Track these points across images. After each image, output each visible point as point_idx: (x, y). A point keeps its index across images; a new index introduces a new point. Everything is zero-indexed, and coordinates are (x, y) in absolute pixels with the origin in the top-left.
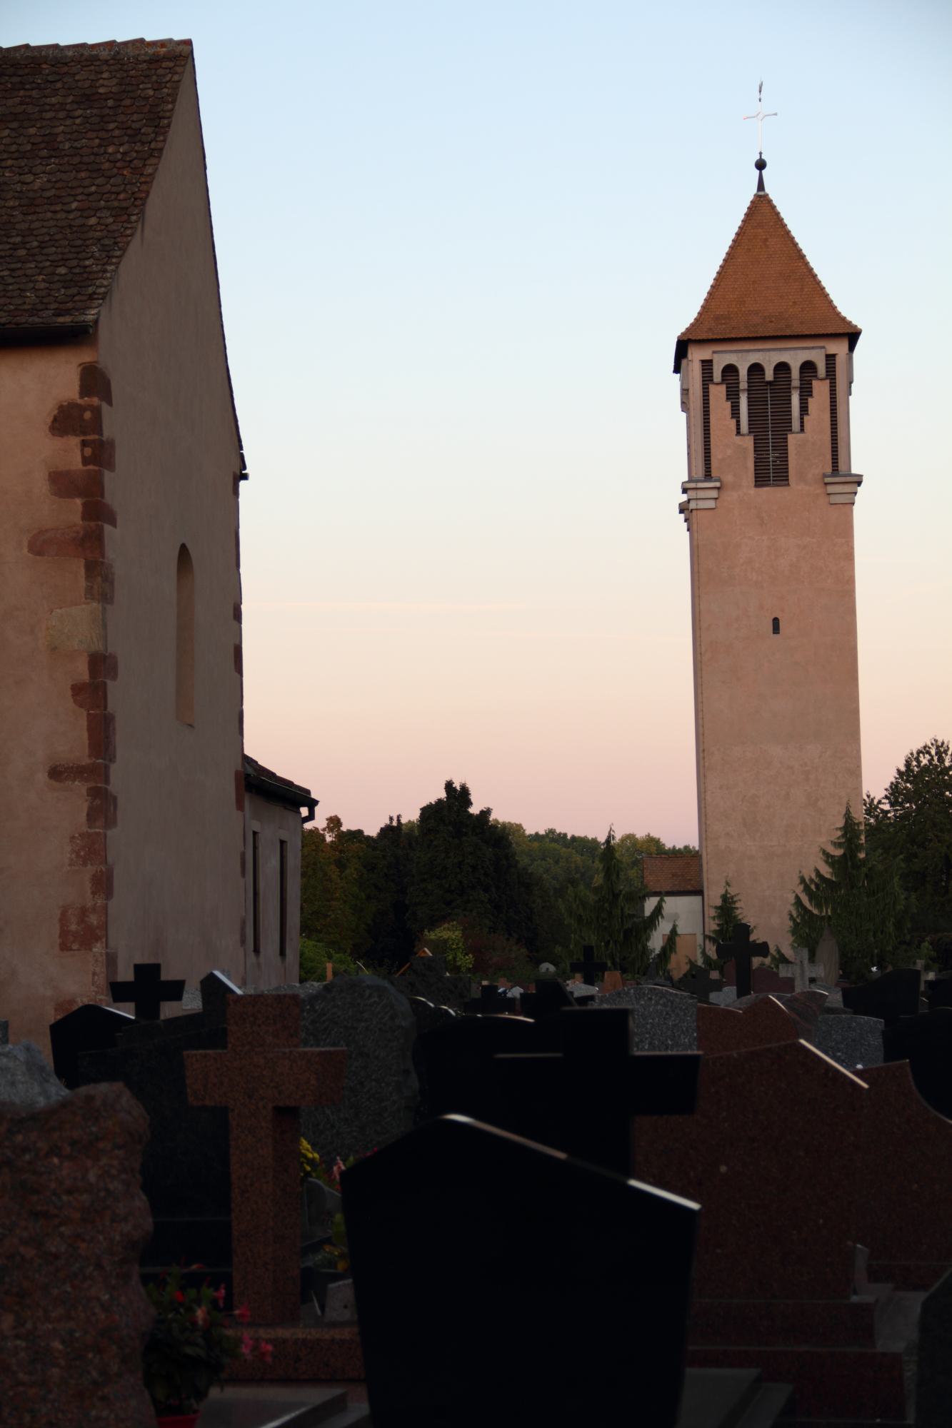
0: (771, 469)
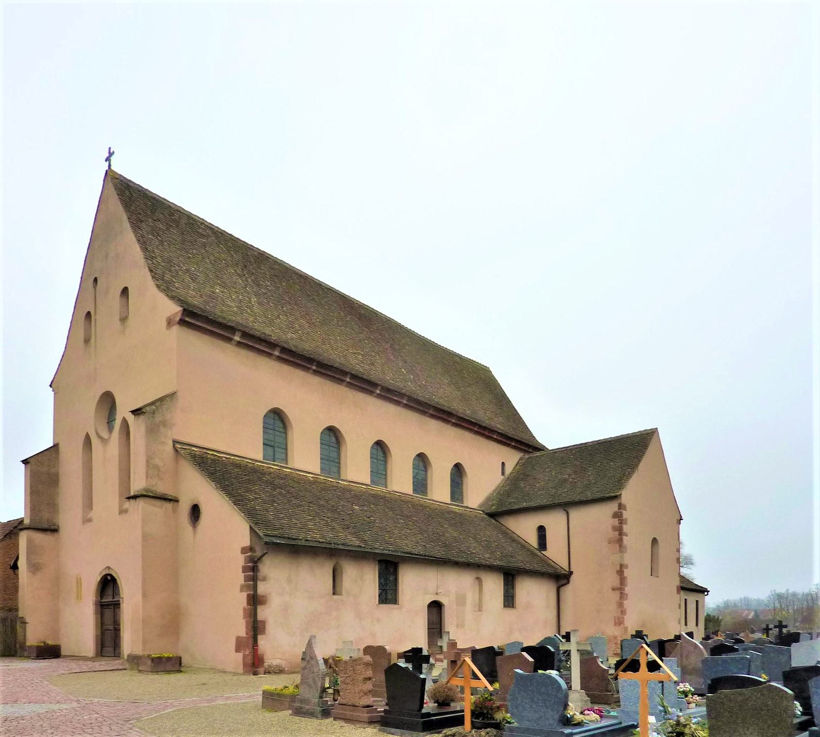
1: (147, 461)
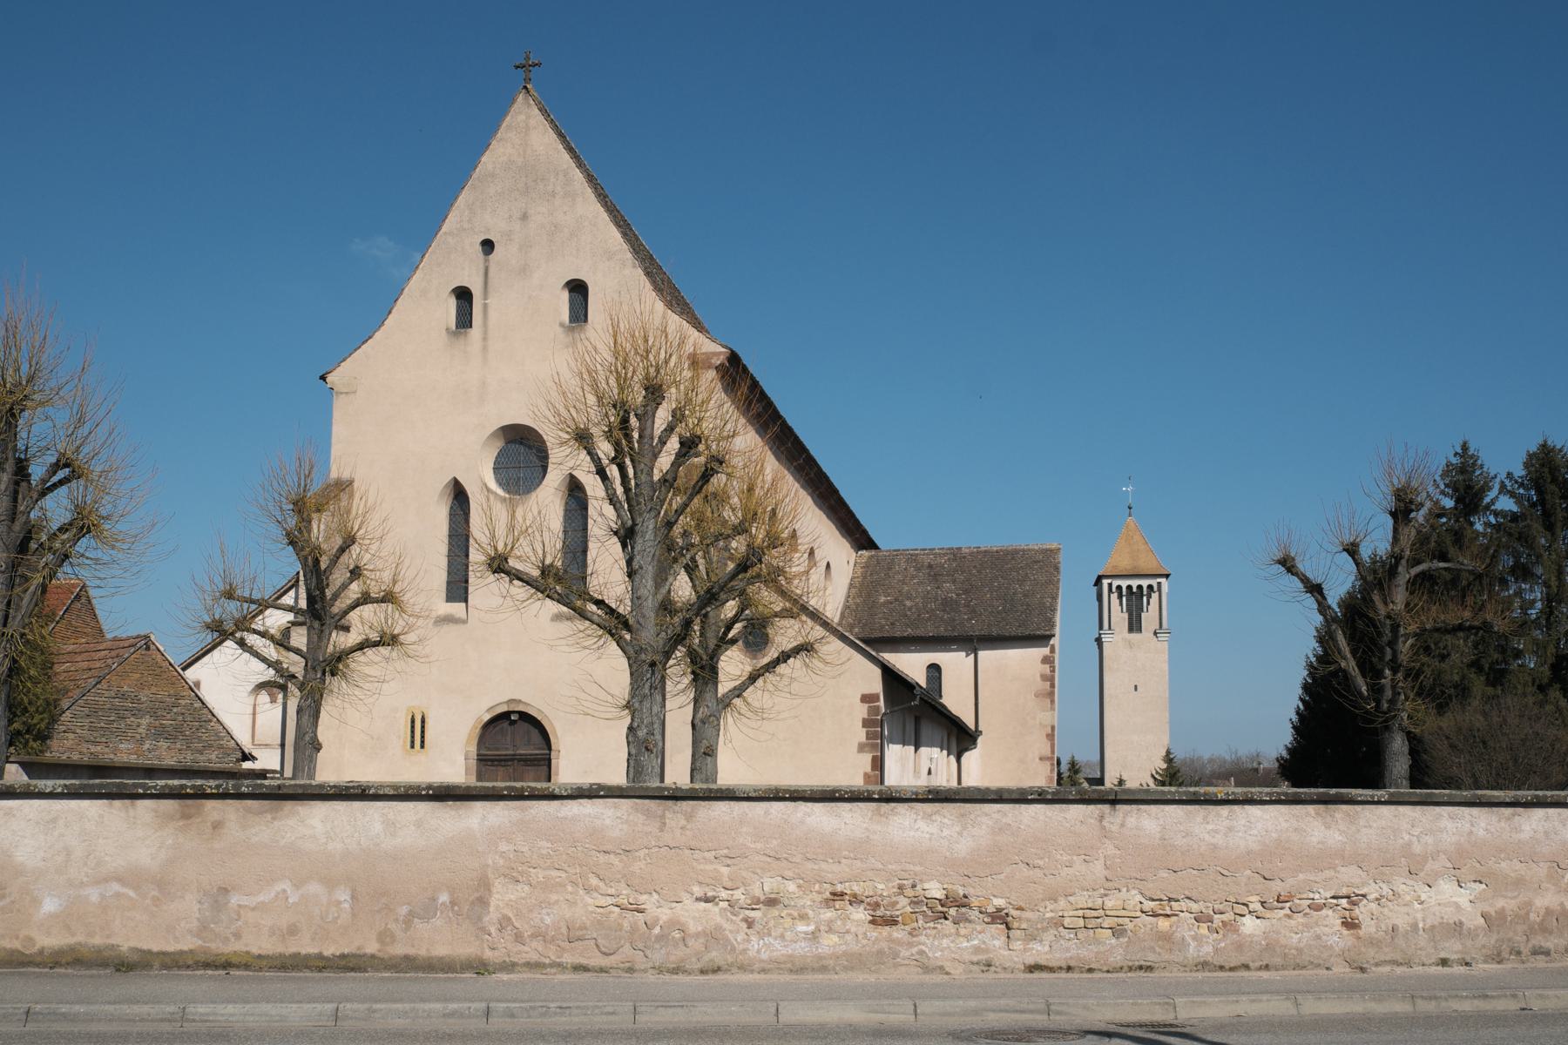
0: (1135, 625)
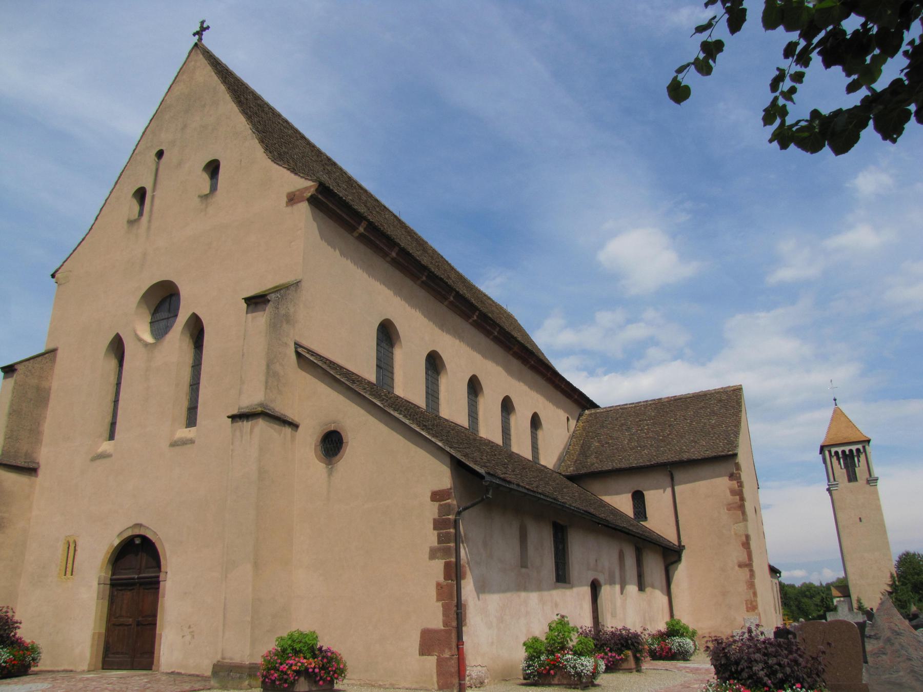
0: (852, 477)
1: (268, 366)
